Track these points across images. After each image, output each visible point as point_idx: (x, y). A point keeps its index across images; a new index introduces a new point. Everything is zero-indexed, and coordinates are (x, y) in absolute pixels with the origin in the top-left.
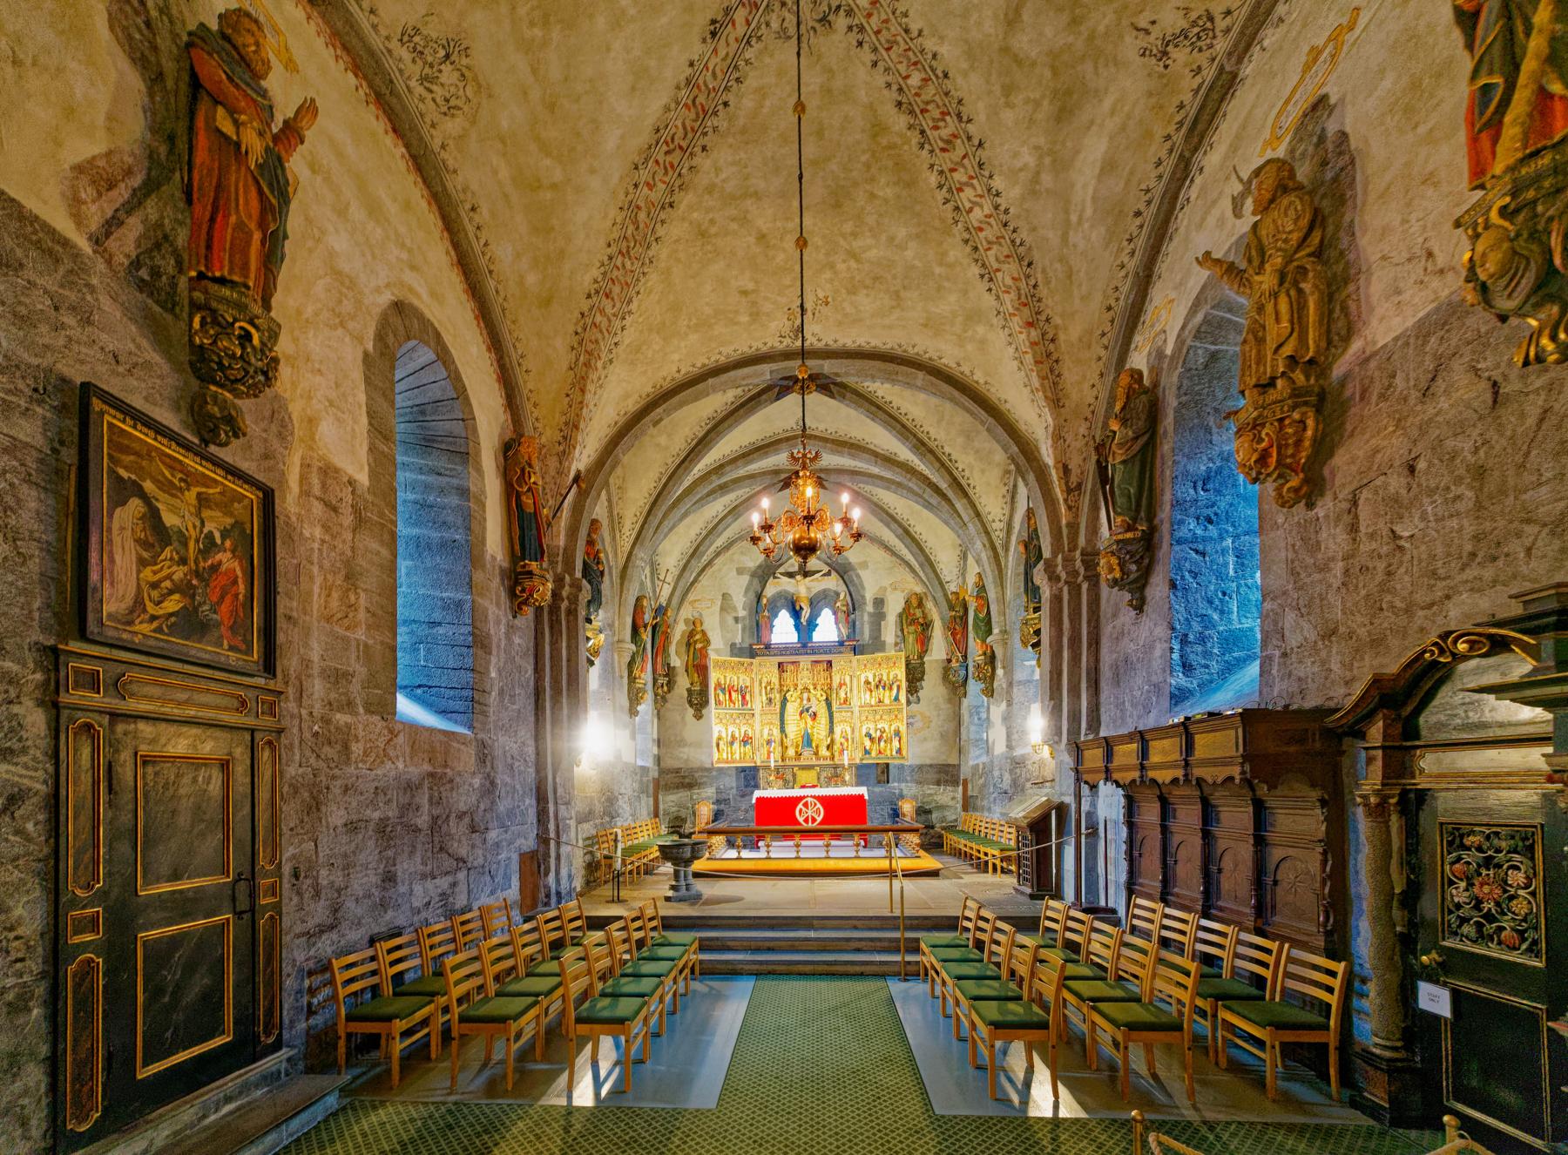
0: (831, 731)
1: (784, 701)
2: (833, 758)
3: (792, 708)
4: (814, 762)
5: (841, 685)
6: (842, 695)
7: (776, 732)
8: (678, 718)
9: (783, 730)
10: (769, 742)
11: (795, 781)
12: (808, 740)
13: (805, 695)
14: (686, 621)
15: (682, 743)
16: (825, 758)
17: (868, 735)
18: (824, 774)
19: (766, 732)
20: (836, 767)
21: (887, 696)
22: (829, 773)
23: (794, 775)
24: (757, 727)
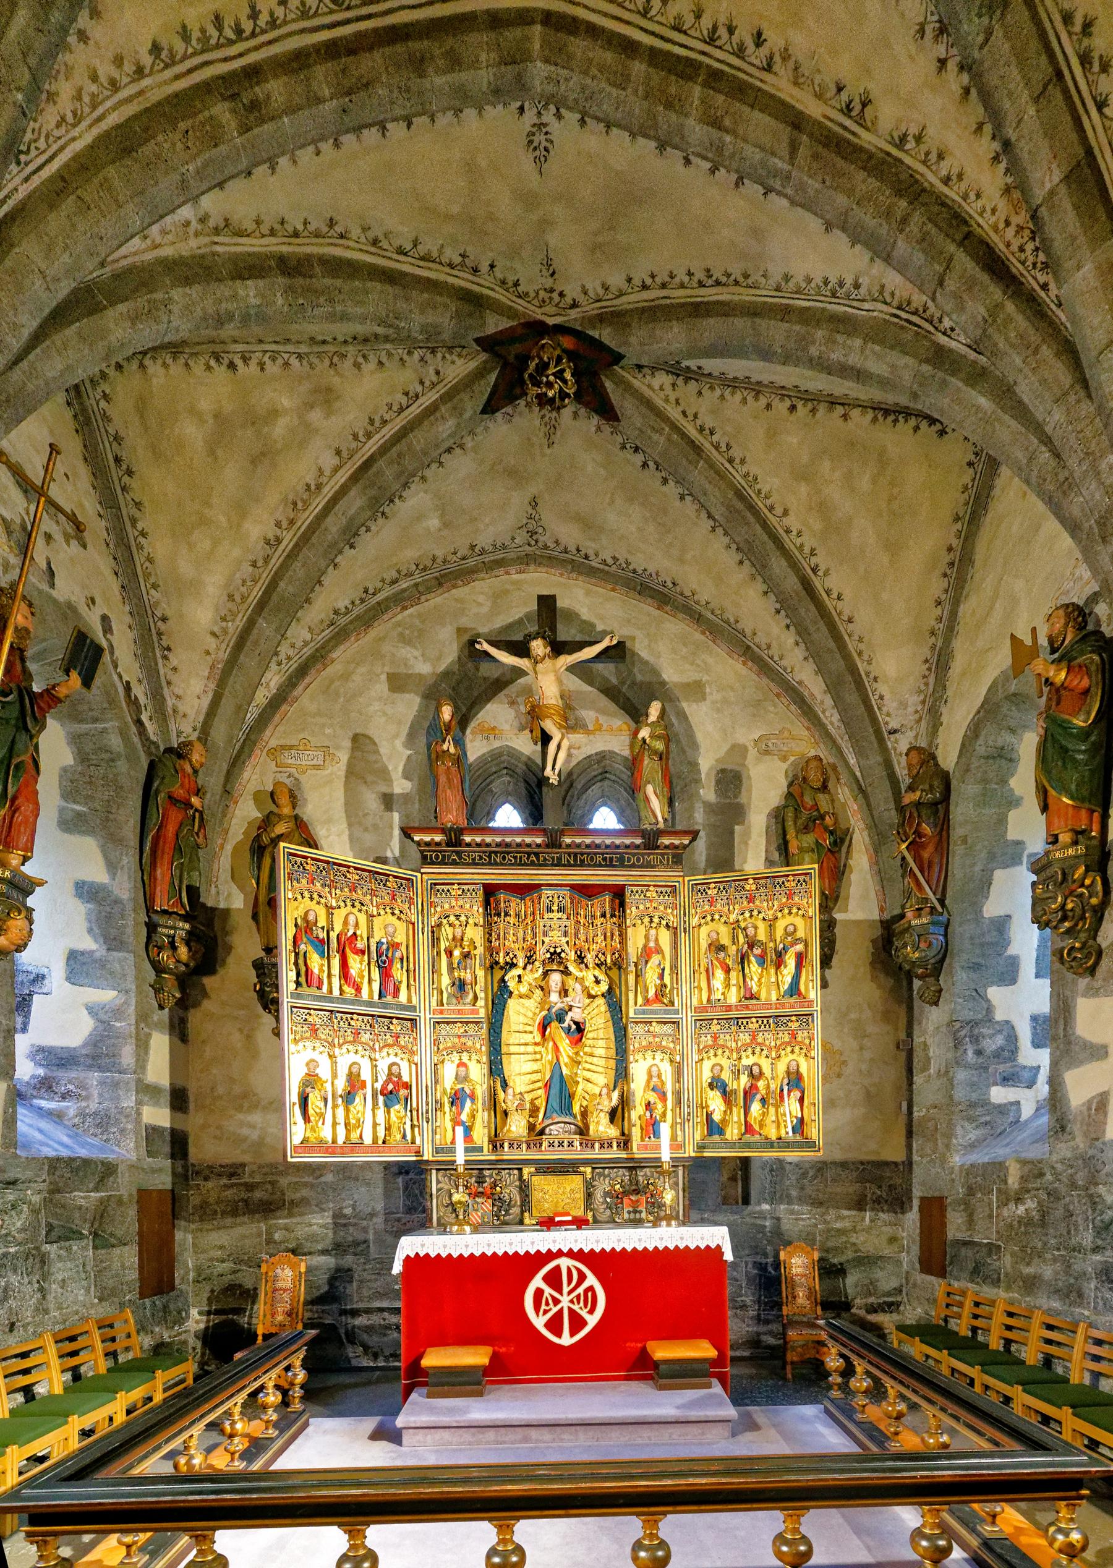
0: (622, 1073)
1: (500, 997)
2: (625, 1142)
3: (521, 1014)
4: (577, 1152)
5: (647, 953)
6: (651, 977)
7: (478, 1072)
8: (237, 1038)
9: (495, 1068)
10: (457, 1099)
11: (525, 1205)
12: (560, 1091)
13: (555, 979)
14: (257, 796)
15: (246, 1100)
16: (605, 1144)
17: (716, 1084)
18: (602, 1186)
19: (449, 1072)
20: (634, 1166)
21: (769, 985)
22: (618, 1179)
23: (524, 1188)
24: (426, 1055)
